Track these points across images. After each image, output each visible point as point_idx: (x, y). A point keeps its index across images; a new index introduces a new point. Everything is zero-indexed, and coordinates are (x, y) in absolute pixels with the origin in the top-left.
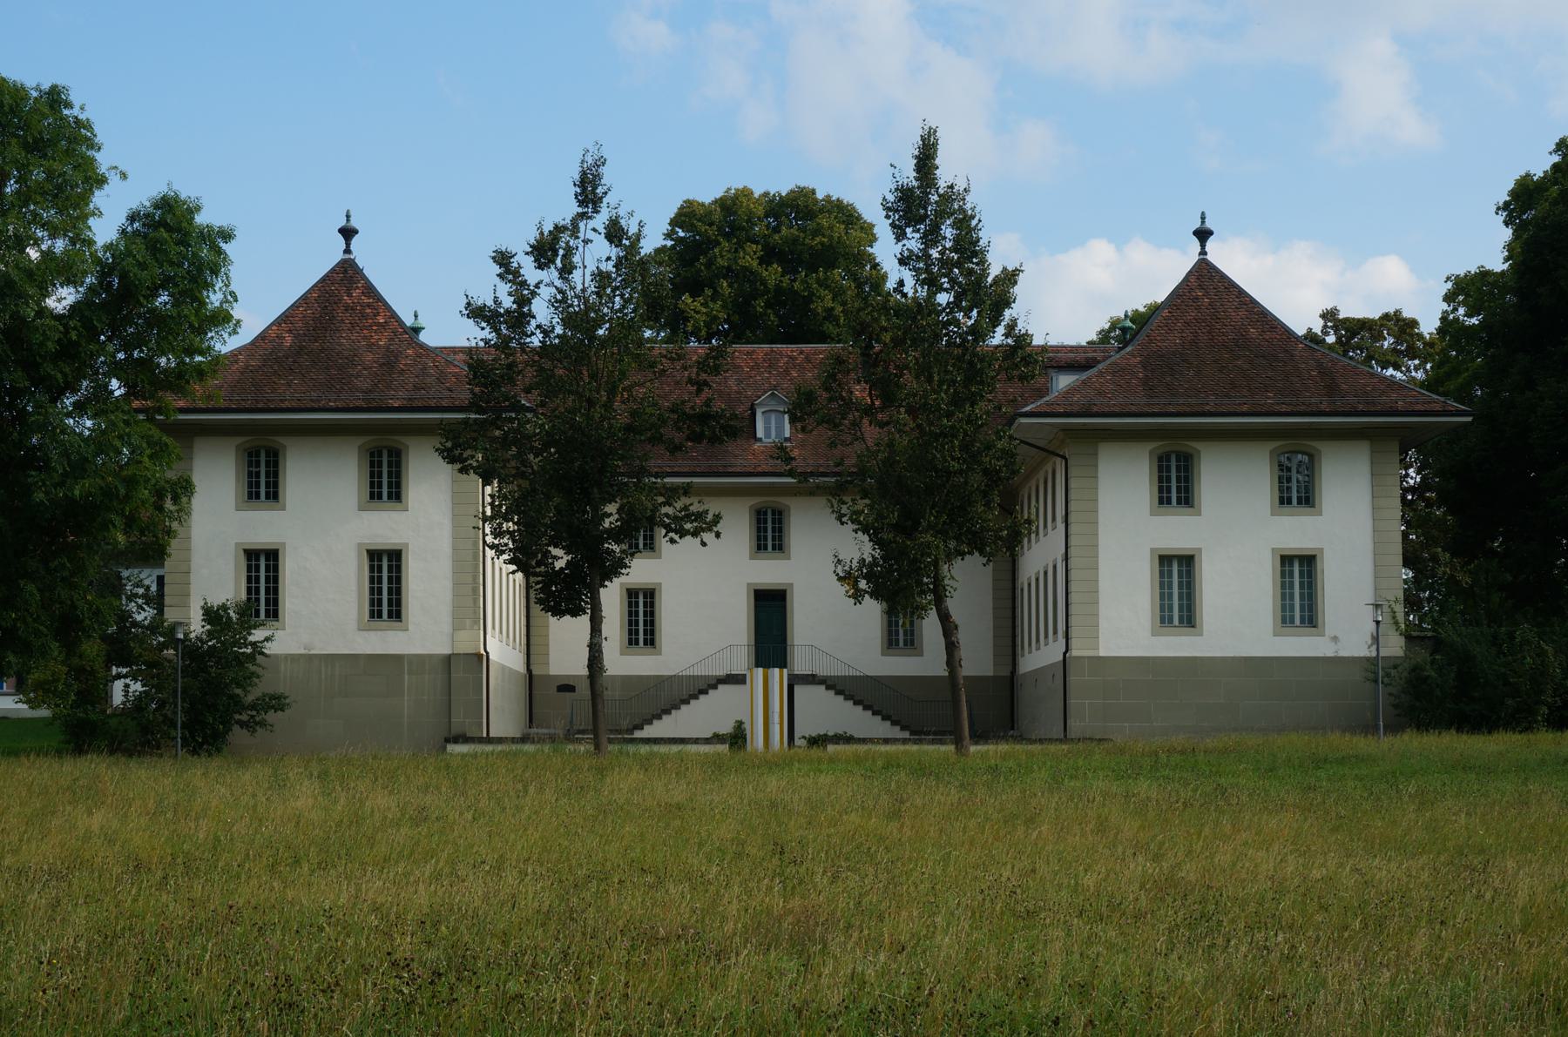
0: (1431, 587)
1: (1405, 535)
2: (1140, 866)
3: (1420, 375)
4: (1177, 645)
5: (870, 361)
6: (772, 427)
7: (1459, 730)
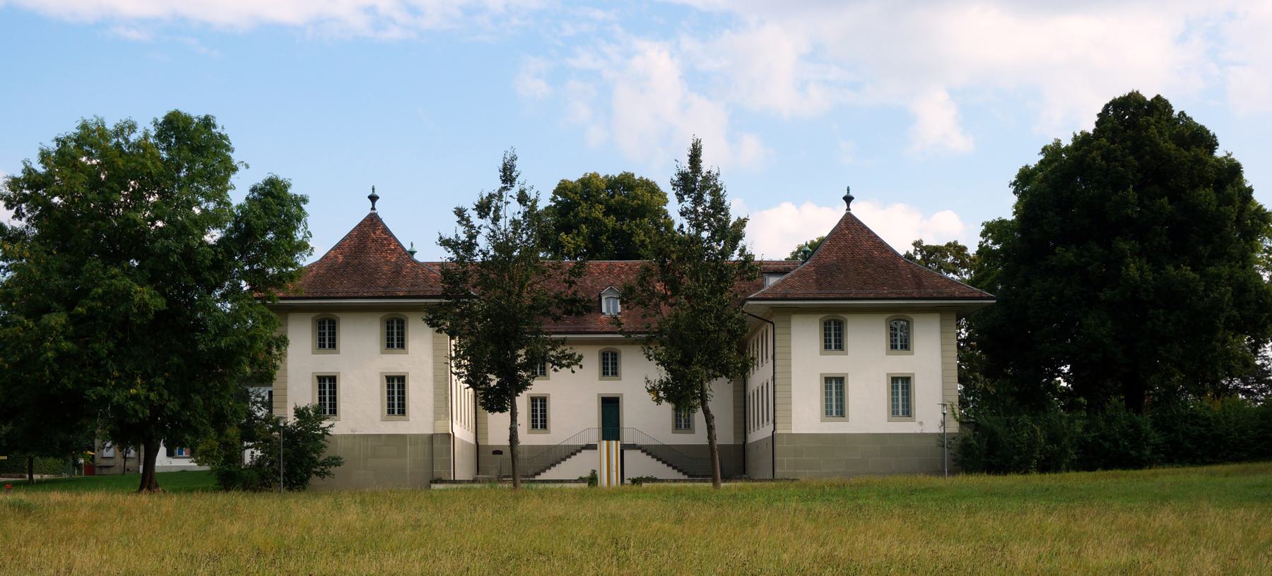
0: (974, 395)
1: (959, 366)
2: (811, 549)
3: (967, 277)
4: (835, 427)
5: (664, 269)
6: (610, 307)
7: (989, 473)
